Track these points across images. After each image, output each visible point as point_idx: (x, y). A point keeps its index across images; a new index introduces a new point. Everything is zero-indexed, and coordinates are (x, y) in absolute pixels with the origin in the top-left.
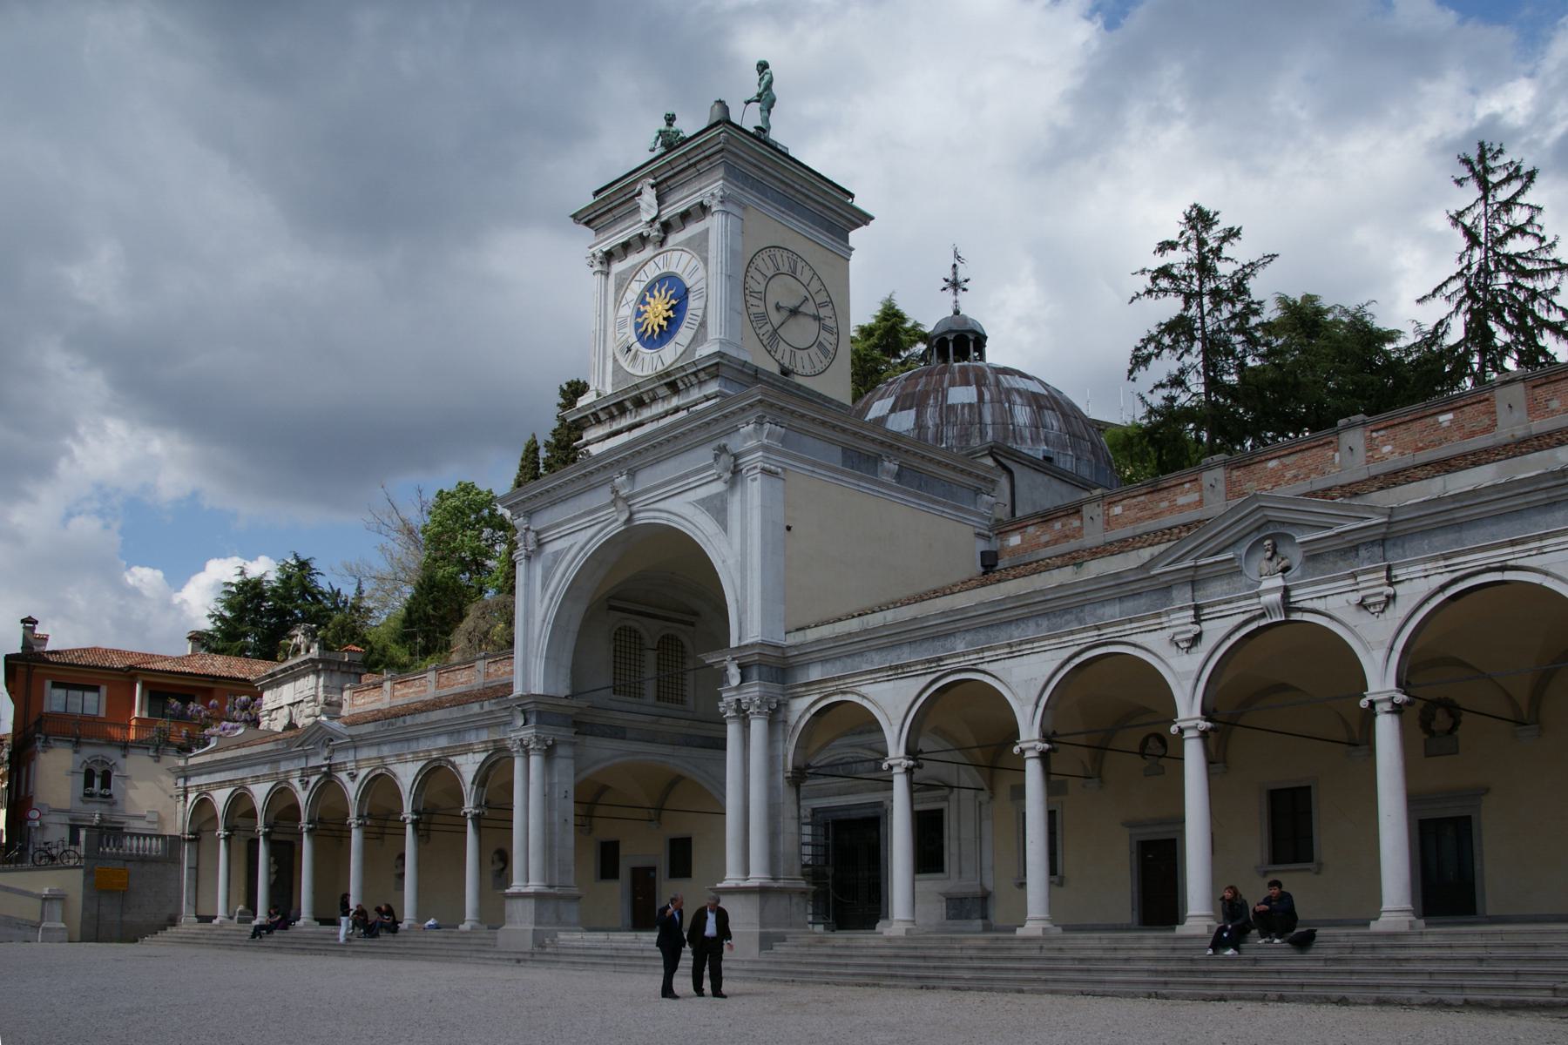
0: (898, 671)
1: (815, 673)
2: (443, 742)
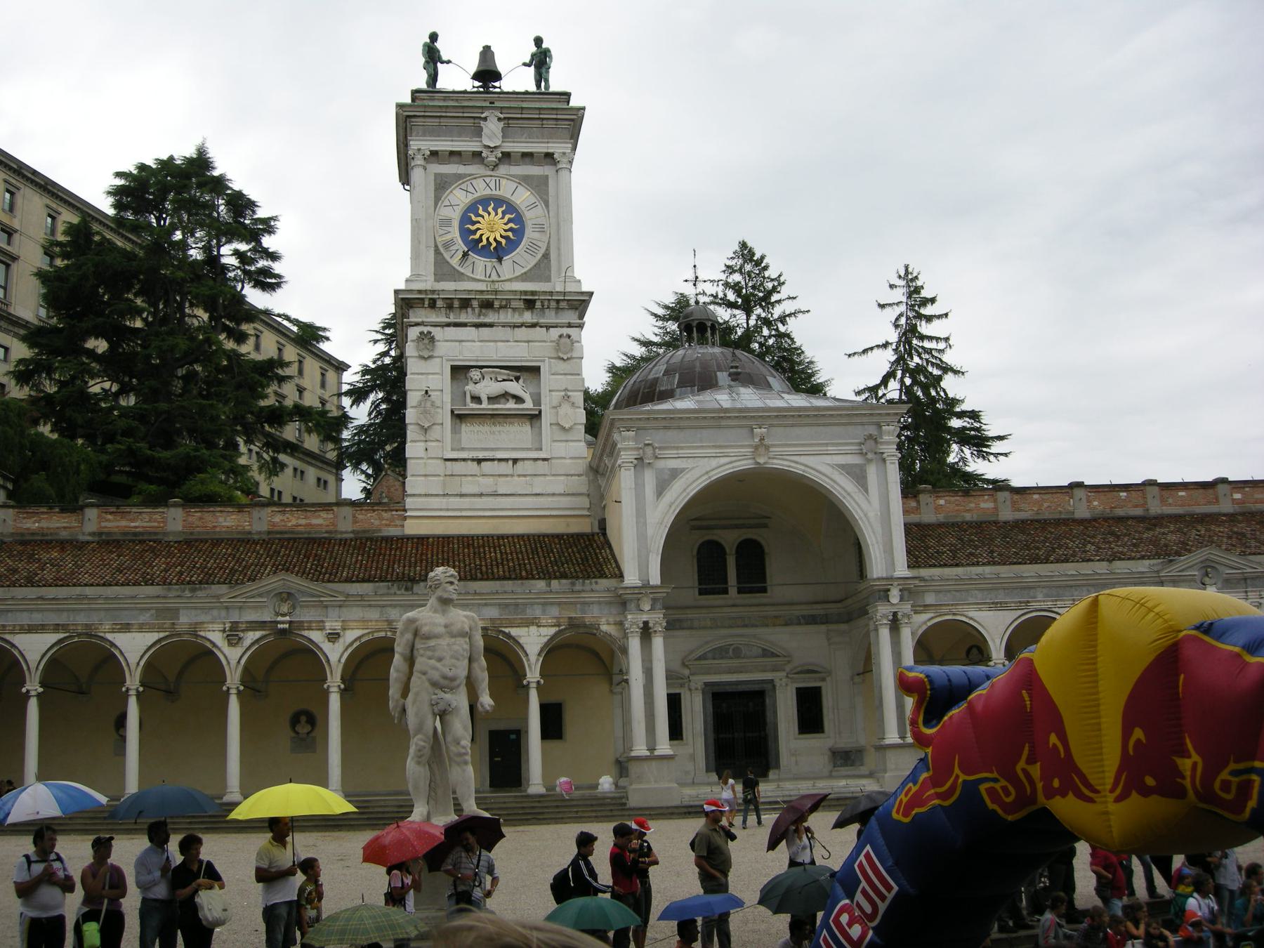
0: (997, 606)
1: (930, 599)
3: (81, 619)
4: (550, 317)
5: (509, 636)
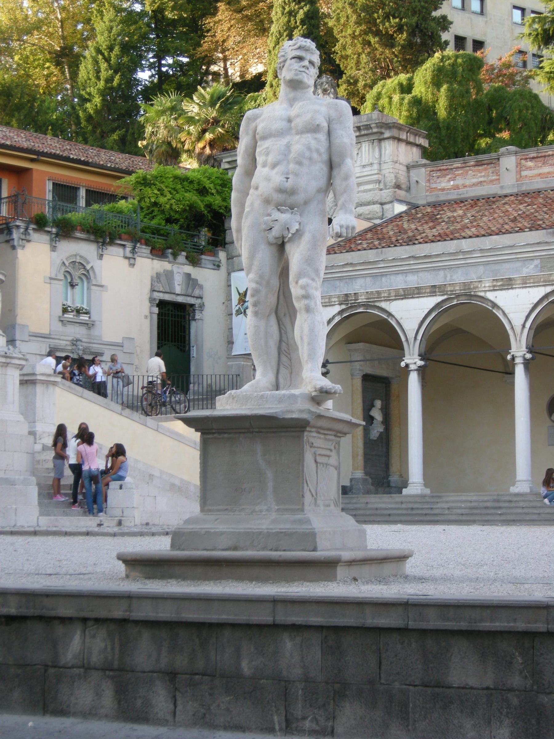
3: (458, 278)
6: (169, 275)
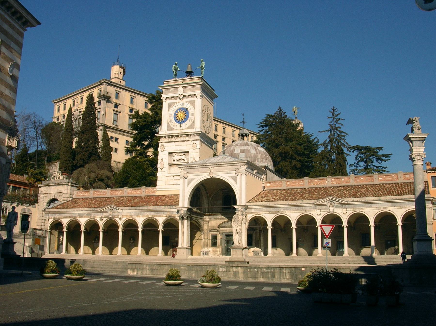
0: (270, 212)
2: (153, 213)
3: (73, 215)
4: (192, 138)
5: (156, 219)
6: (25, 209)
